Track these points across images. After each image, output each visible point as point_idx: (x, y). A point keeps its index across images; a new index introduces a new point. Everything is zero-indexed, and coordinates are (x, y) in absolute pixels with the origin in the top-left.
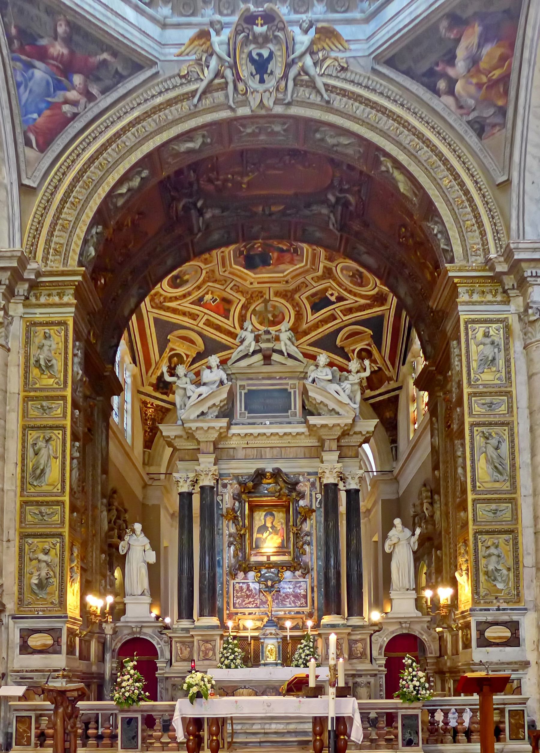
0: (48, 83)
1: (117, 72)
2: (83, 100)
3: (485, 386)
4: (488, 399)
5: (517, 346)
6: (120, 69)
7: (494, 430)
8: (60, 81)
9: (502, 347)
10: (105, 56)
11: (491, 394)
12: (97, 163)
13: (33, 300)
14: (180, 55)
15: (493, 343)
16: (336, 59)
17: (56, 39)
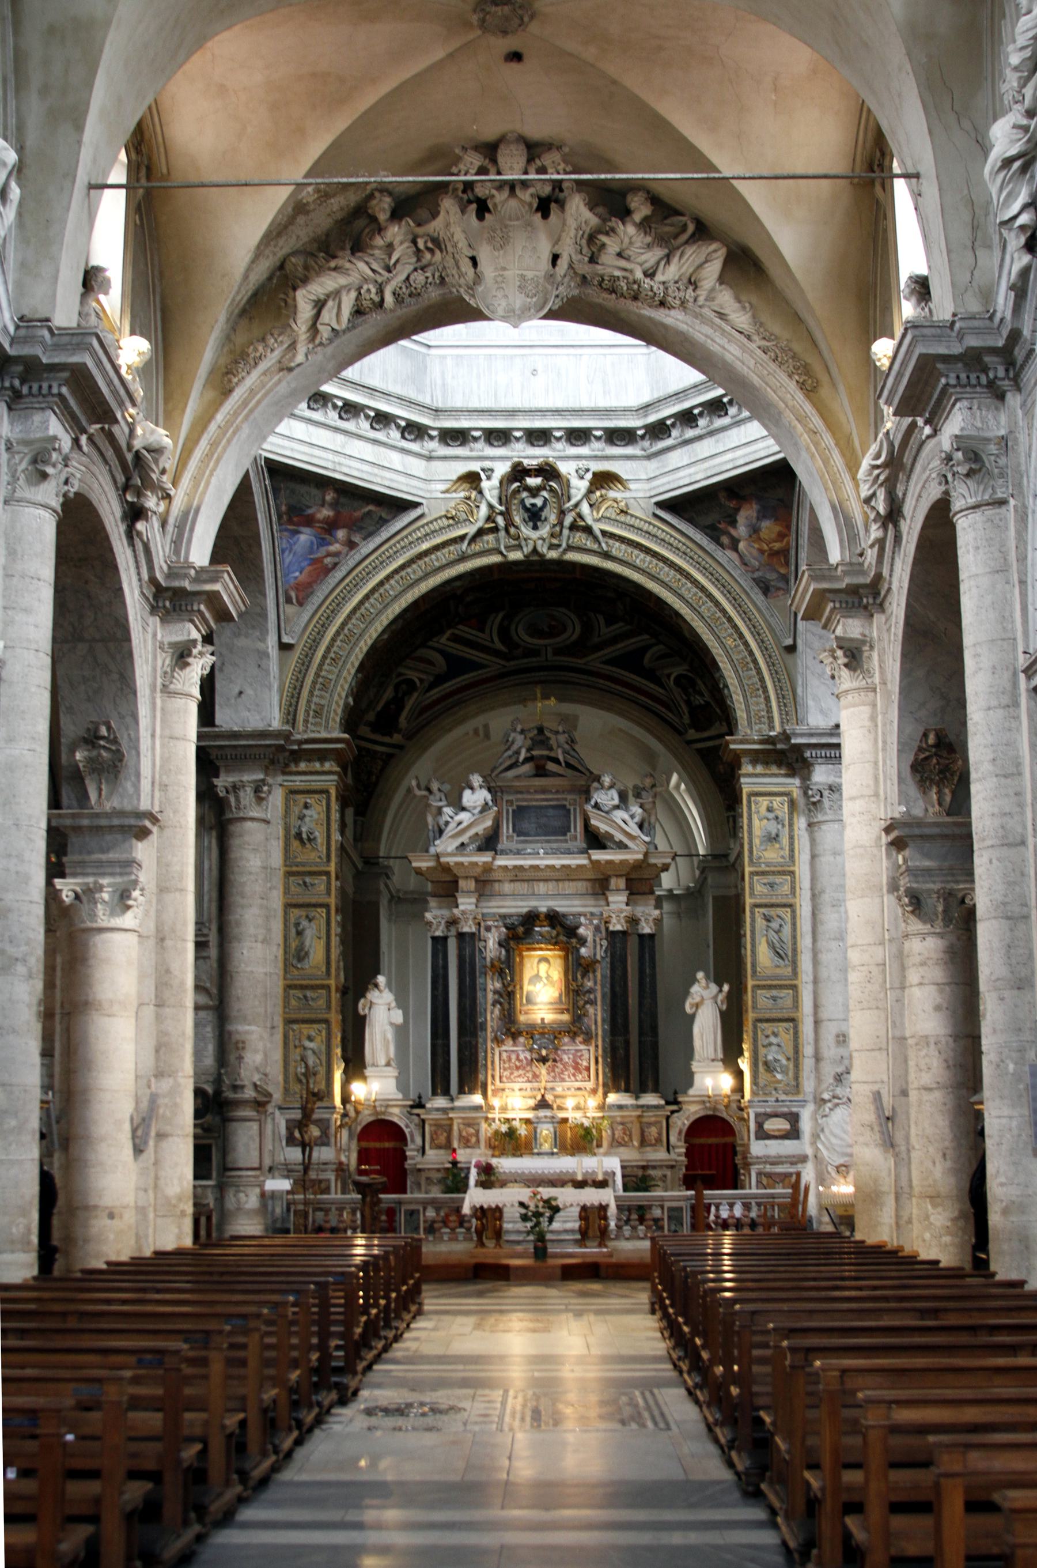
0: (312, 543)
1: (381, 518)
2: (345, 549)
3: (768, 865)
4: (771, 879)
5: (801, 823)
6: (384, 515)
7: (772, 912)
8: (323, 539)
9: (787, 823)
10: (371, 507)
11: (773, 873)
12: (358, 615)
13: (293, 768)
14: (447, 491)
15: (777, 818)
16: (615, 500)
17: (323, 505)
